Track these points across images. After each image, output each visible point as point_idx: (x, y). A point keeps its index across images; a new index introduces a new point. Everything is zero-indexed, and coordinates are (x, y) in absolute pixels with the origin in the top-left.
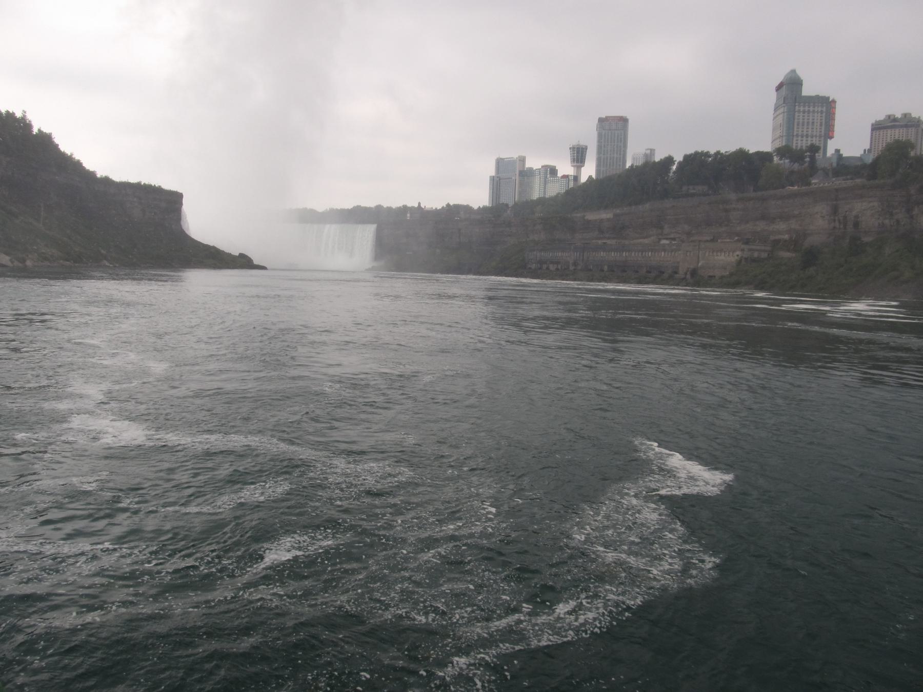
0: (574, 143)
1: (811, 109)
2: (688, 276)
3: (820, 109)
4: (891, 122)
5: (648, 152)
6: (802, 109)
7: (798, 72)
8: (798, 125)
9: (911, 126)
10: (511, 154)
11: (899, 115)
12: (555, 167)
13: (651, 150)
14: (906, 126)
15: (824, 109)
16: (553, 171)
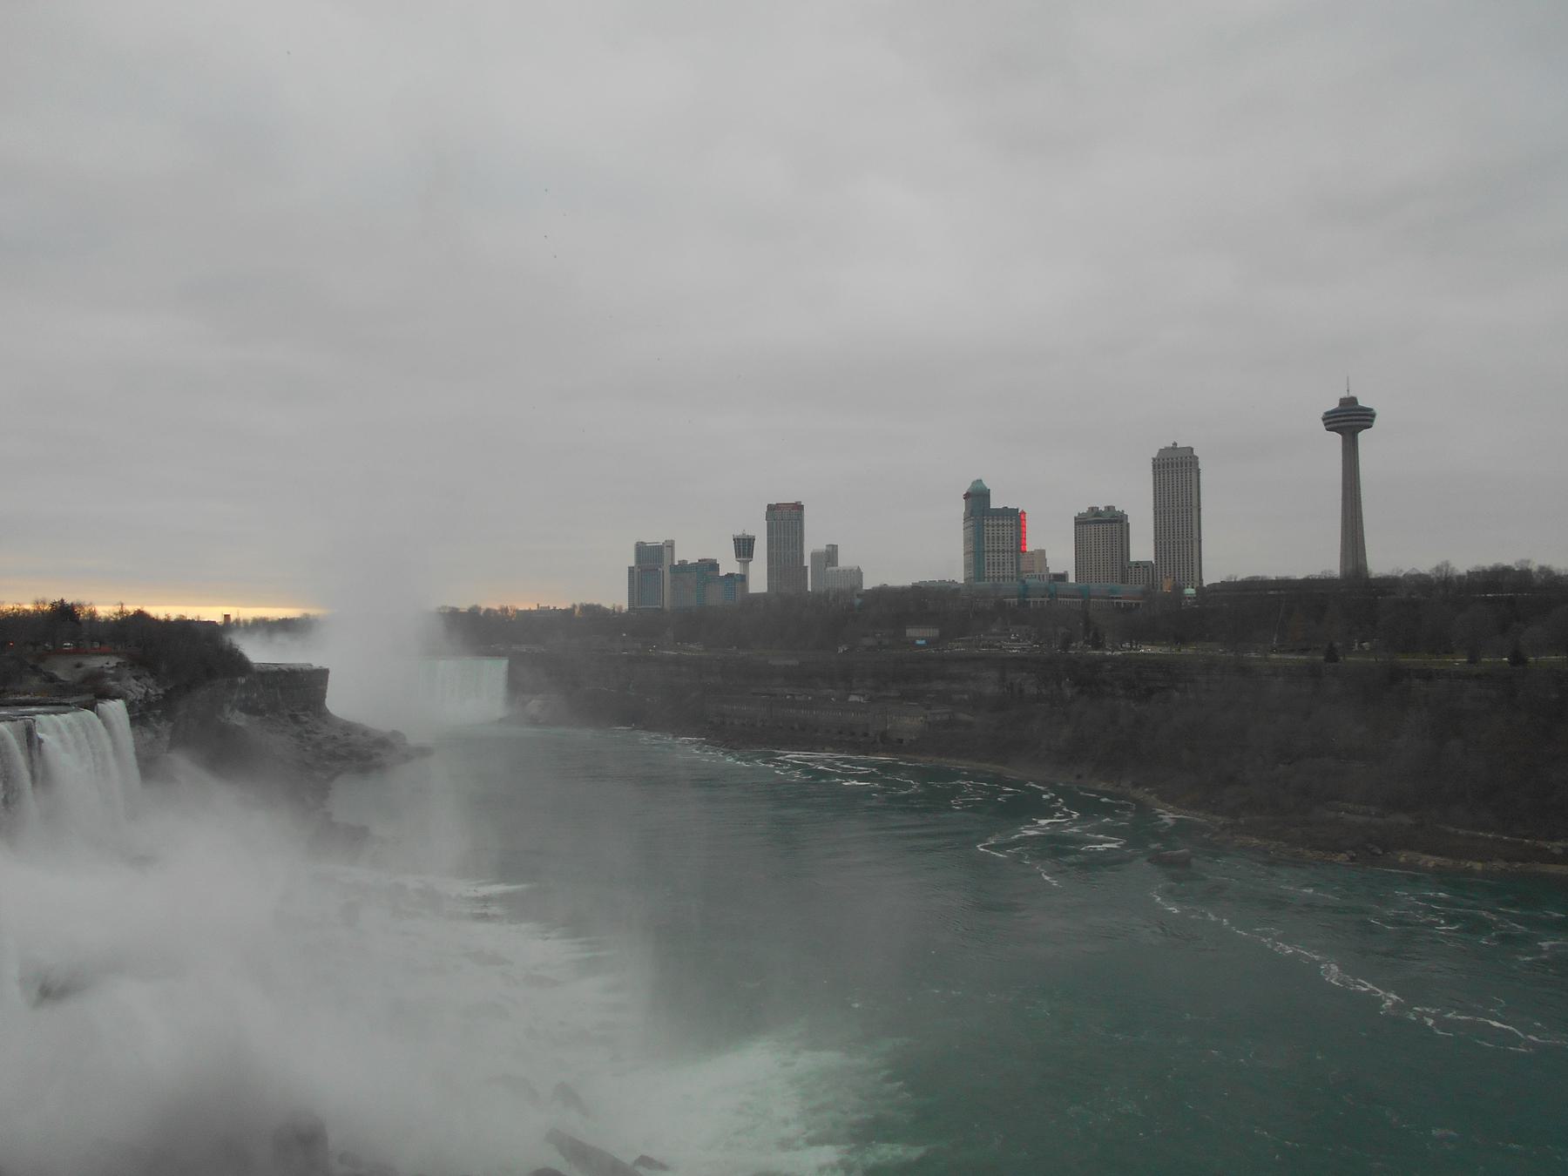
0: (739, 533)
1: (1001, 522)
2: (878, 740)
3: (1009, 522)
4: (1095, 516)
5: (830, 549)
6: (990, 522)
7: (984, 483)
8: (988, 540)
9: (1116, 521)
10: (654, 537)
11: (1102, 508)
12: (716, 560)
13: (833, 546)
14: (1110, 522)
15: (1014, 522)
16: (713, 566)
